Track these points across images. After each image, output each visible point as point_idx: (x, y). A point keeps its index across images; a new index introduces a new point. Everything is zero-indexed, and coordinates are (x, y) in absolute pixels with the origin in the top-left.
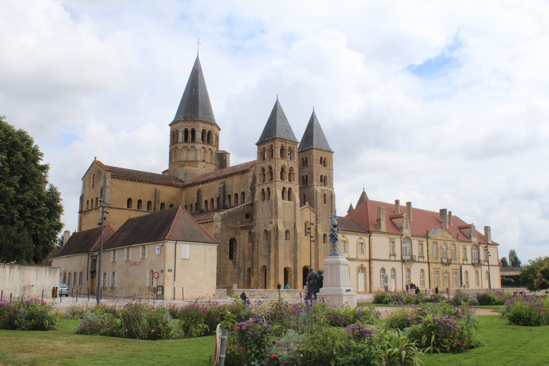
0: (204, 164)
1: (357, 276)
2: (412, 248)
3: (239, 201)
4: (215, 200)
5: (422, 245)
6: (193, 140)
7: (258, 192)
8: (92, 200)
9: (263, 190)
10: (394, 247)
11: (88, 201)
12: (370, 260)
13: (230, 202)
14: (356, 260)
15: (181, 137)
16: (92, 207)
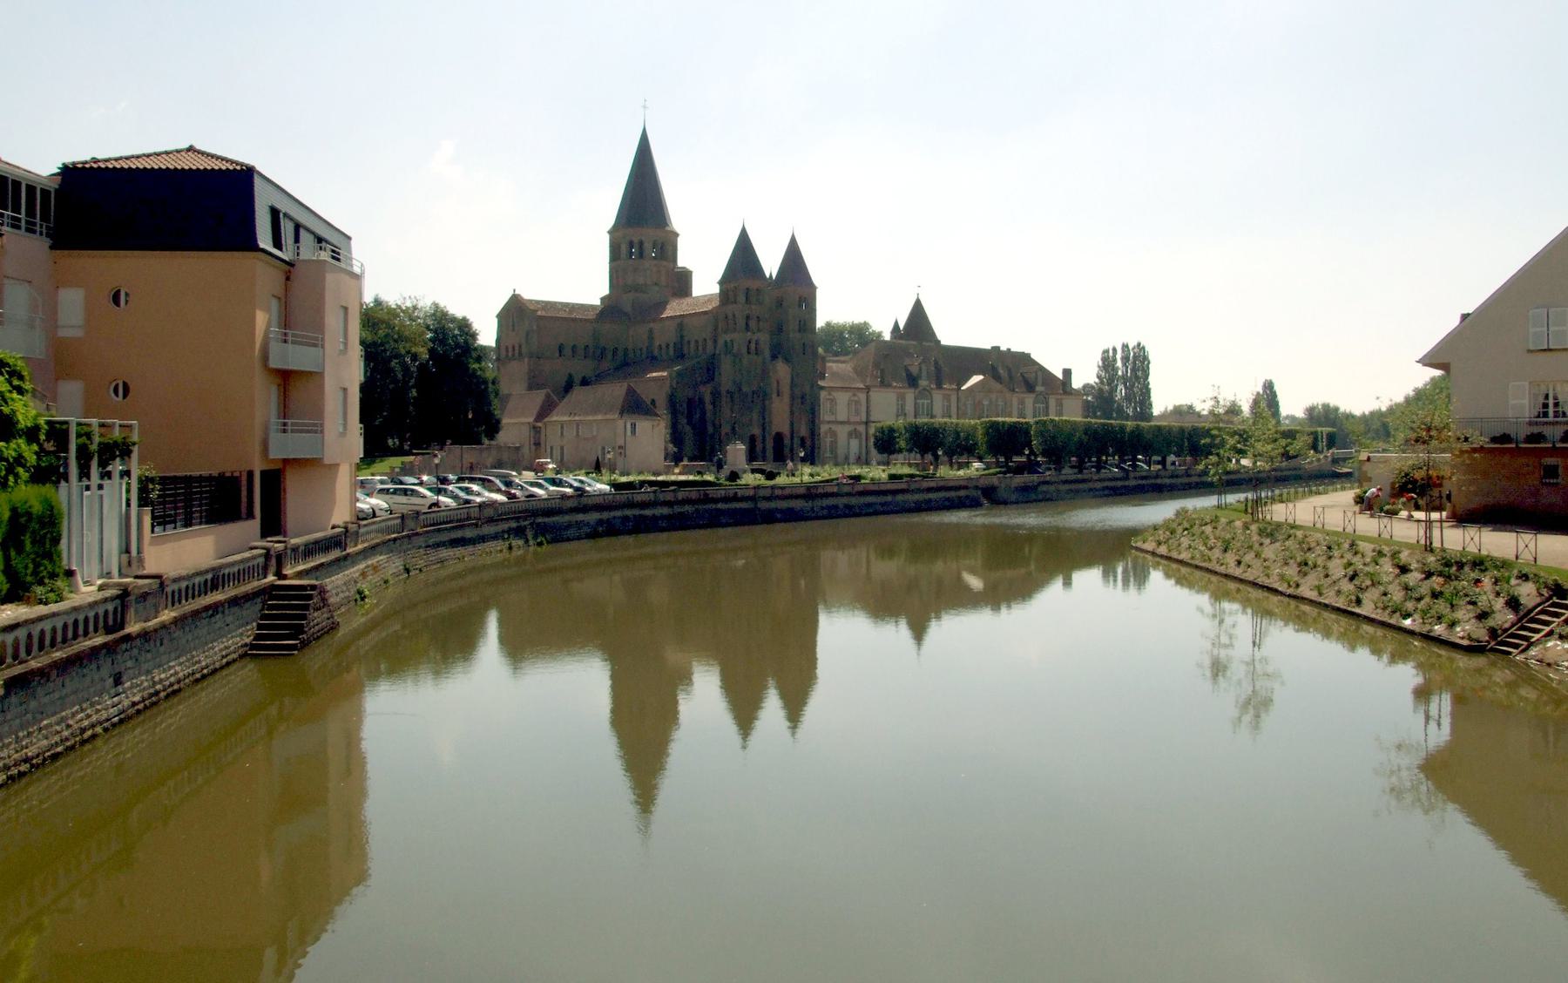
0: (657, 288)
1: (849, 443)
2: (932, 405)
3: (700, 348)
4: (672, 345)
5: (949, 401)
6: (641, 255)
7: (721, 342)
8: (514, 347)
9: (726, 342)
10: (903, 406)
11: (507, 348)
12: (867, 423)
13: (689, 348)
14: (848, 422)
15: (625, 252)
16: (513, 355)
